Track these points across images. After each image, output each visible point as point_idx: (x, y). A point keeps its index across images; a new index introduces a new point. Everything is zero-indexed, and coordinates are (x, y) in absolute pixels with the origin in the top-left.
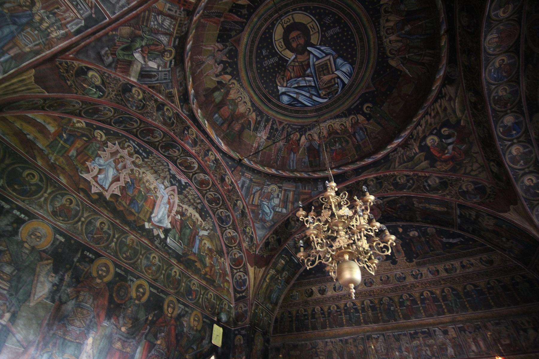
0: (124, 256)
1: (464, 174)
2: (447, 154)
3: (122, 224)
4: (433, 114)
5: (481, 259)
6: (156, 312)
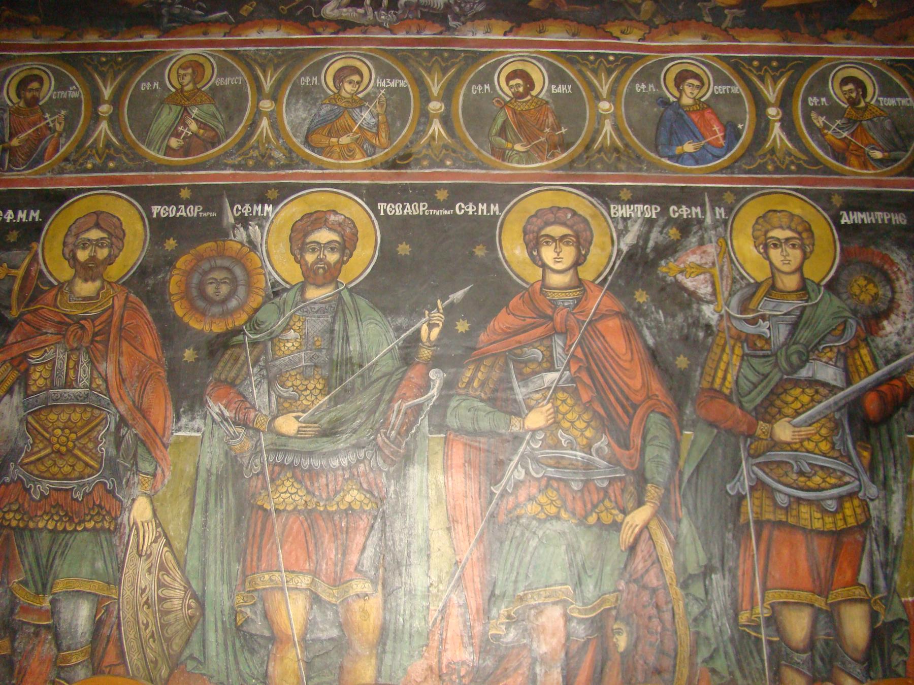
0: (174, 143)
3: (115, 35)
6: (458, 295)
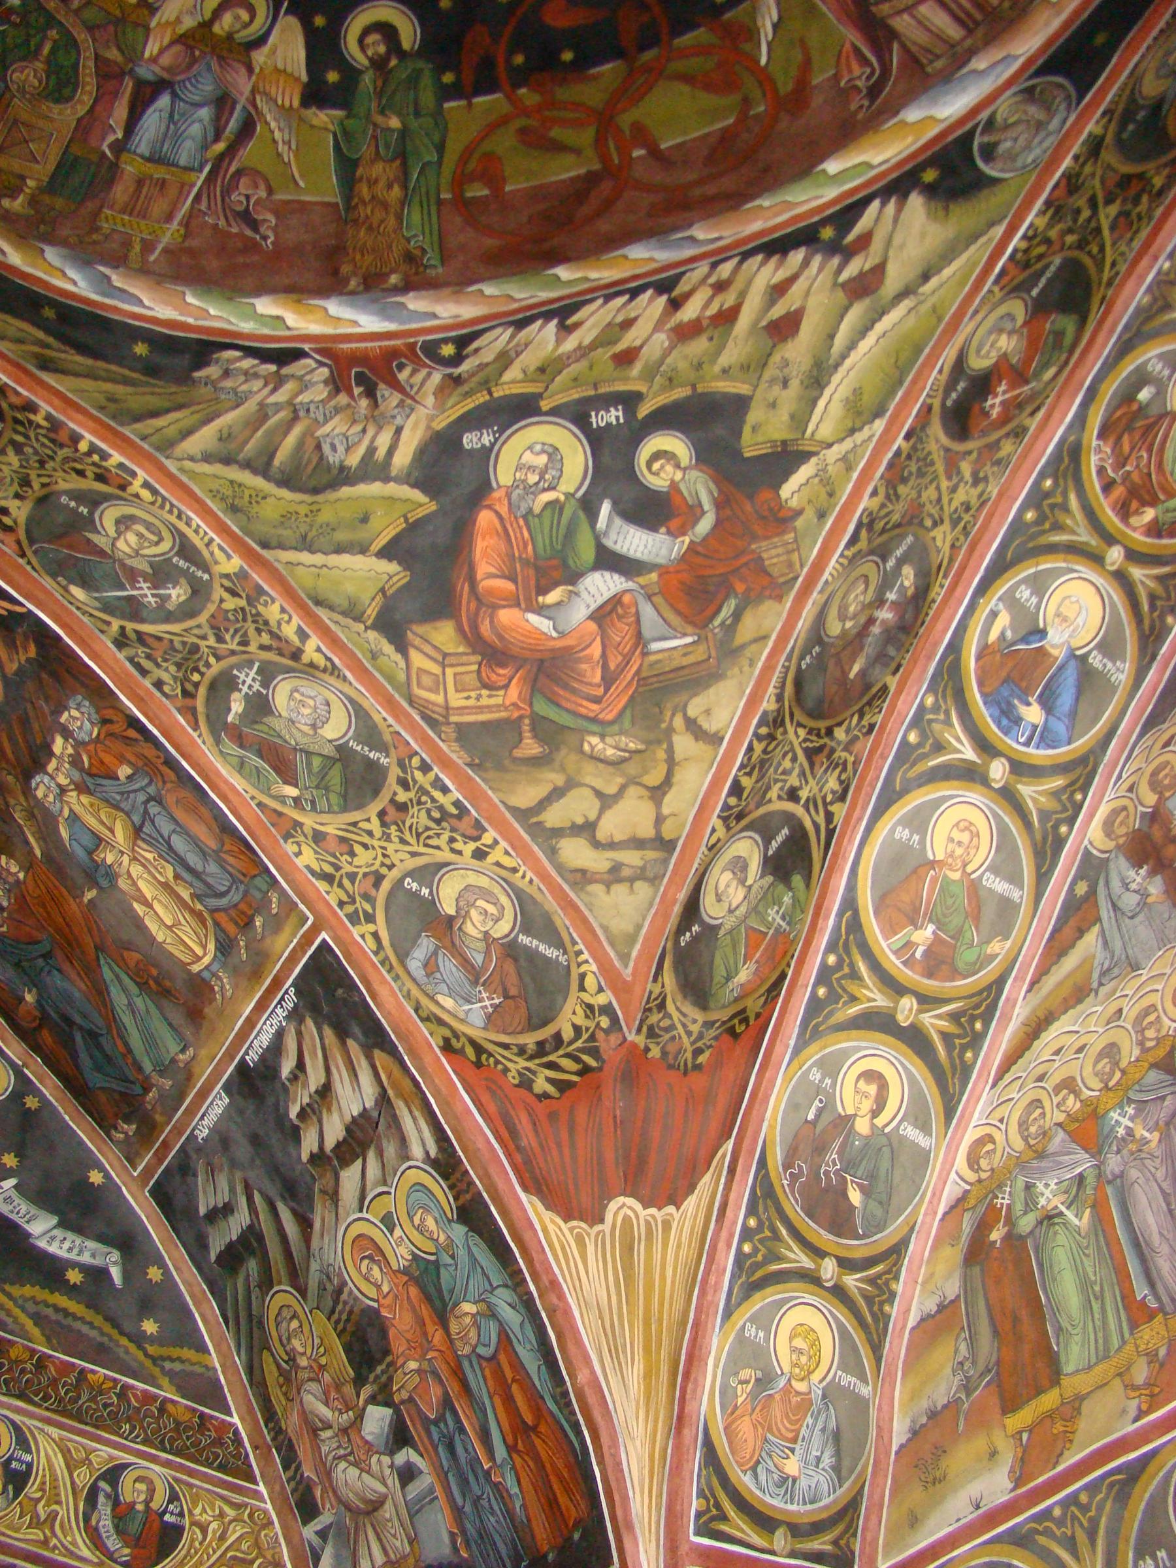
1: (523, 814)
2: (540, 610)
4: (690, 312)
5: (114, 1474)
